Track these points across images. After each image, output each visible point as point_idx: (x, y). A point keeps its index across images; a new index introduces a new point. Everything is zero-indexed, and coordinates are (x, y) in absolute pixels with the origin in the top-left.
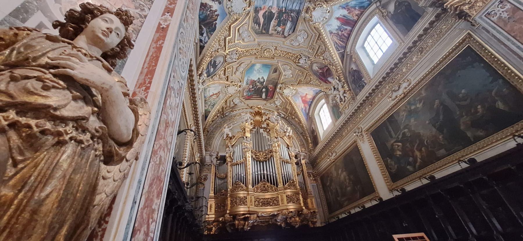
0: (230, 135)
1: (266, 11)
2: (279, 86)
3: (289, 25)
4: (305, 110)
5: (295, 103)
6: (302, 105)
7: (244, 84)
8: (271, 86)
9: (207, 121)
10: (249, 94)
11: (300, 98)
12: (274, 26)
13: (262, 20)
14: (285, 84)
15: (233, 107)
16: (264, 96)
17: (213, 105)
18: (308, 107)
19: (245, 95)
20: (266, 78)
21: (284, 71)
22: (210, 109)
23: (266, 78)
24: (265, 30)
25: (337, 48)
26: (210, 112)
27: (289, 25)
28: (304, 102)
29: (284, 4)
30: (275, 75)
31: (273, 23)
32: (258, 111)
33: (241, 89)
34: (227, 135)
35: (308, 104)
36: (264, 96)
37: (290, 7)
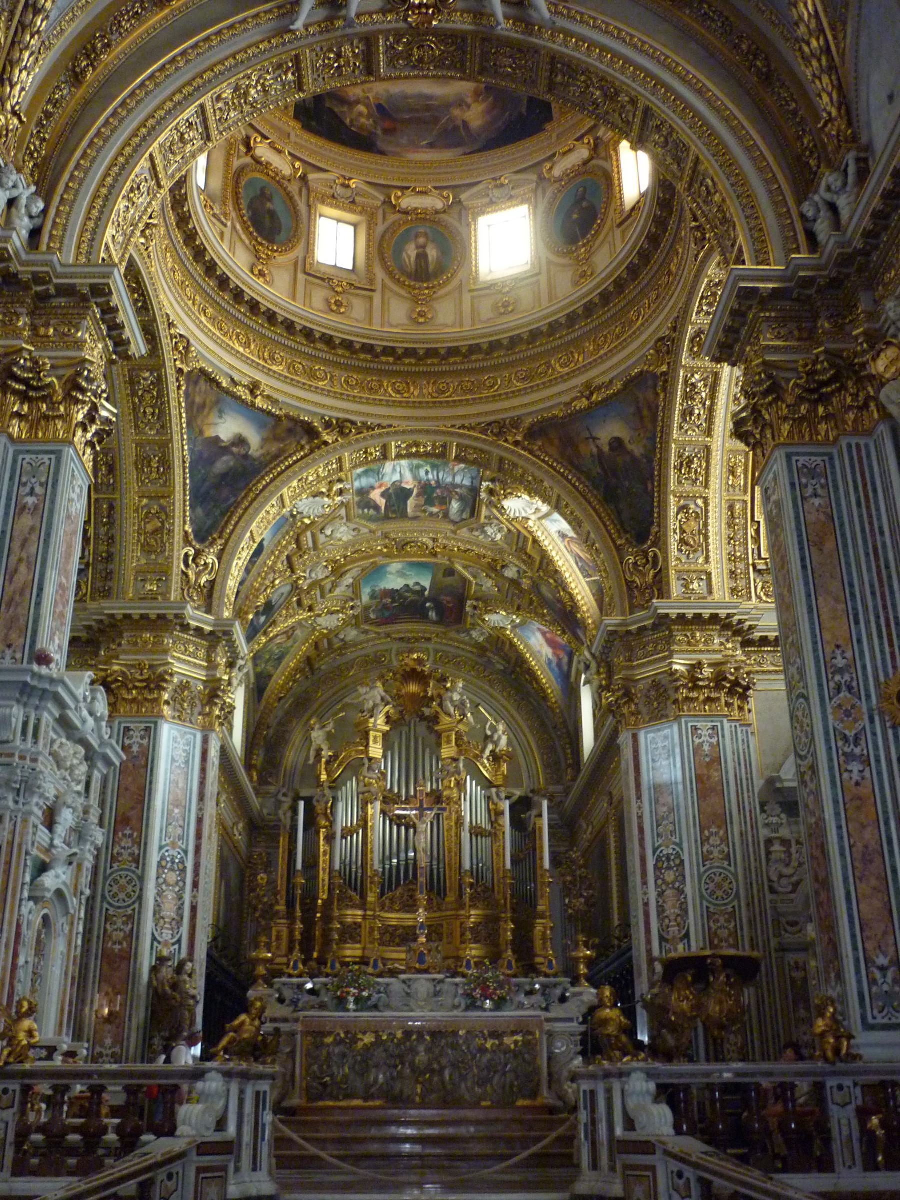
0: (327, 753)
1: (388, 490)
2: (469, 603)
3: (455, 506)
4: (559, 665)
5: (526, 646)
6: (547, 651)
7: (366, 598)
8: (449, 599)
9: (264, 702)
10: (387, 614)
11: (539, 635)
12: (416, 506)
13: (382, 503)
14: (485, 602)
15: (340, 649)
16: (433, 615)
17: (280, 659)
18: (566, 660)
19: (372, 616)
20: (426, 583)
21: (475, 577)
22: (270, 668)
23: (426, 583)
24: (394, 512)
25: (582, 570)
26: (270, 677)
27: (455, 506)
28: (551, 643)
29: (430, 477)
30: (449, 580)
31: (411, 503)
32: (414, 670)
33: (356, 612)
34: (319, 751)
35: (564, 650)
36: (433, 615)
37: (449, 480)
